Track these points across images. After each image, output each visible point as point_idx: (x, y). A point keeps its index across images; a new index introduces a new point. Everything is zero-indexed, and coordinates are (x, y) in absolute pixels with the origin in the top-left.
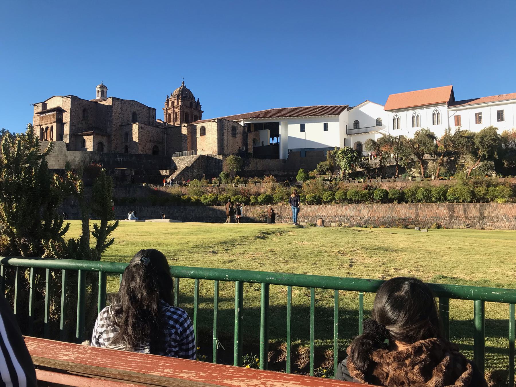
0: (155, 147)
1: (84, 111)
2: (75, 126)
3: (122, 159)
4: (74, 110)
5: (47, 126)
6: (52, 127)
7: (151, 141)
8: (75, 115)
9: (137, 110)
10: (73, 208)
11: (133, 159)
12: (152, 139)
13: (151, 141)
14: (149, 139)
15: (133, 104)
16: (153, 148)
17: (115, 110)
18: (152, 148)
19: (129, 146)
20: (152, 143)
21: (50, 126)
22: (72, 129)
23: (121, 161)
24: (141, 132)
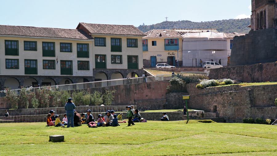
6: (265, 11)
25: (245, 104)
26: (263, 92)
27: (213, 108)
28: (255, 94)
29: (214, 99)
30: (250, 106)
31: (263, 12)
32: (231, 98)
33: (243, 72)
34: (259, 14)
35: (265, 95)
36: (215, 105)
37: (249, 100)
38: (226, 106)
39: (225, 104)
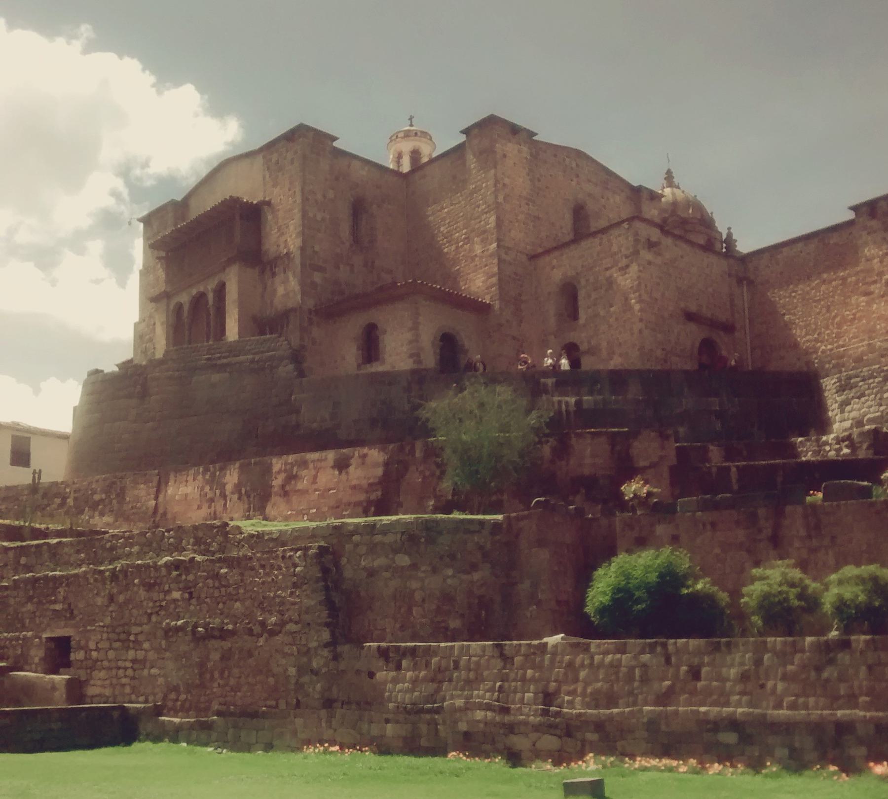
0: (708, 346)
1: (358, 209)
2: (320, 269)
3: (572, 400)
4: (319, 197)
5: (194, 292)
6: (220, 292)
7: (690, 317)
8: (323, 219)
9: (590, 195)
10: (399, 667)
11: (630, 396)
12: (693, 308)
13: (690, 317)
14: (682, 305)
15: (574, 165)
16: (700, 351)
17: (507, 181)
18: (696, 351)
19: (584, 347)
20: (692, 327)
21: (210, 286)
22: (314, 285)
23: (572, 408)
24: (650, 263)
25: (291, 627)
26: (404, 560)
27: (41, 653)
28: (348, 573)
29: (55, 602)
30: (326, 635)
31: (211, 296)
32: (176, 595)
33: (156, 498)
34: (186, 308)
35: (421, 575)
36: (59, 633)
37: (320, 603)
38: (141, 638)
39: (135, 630)
